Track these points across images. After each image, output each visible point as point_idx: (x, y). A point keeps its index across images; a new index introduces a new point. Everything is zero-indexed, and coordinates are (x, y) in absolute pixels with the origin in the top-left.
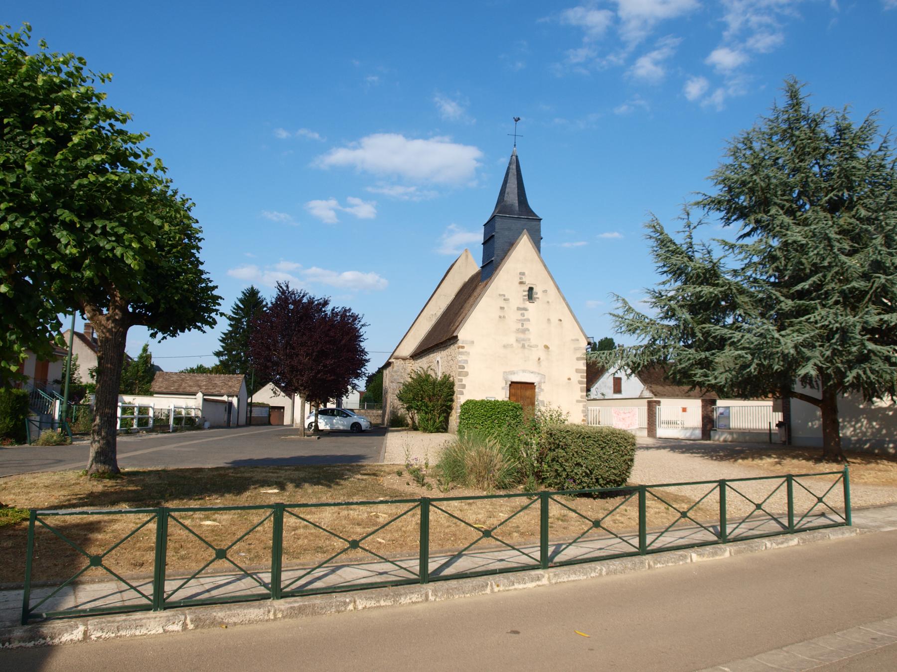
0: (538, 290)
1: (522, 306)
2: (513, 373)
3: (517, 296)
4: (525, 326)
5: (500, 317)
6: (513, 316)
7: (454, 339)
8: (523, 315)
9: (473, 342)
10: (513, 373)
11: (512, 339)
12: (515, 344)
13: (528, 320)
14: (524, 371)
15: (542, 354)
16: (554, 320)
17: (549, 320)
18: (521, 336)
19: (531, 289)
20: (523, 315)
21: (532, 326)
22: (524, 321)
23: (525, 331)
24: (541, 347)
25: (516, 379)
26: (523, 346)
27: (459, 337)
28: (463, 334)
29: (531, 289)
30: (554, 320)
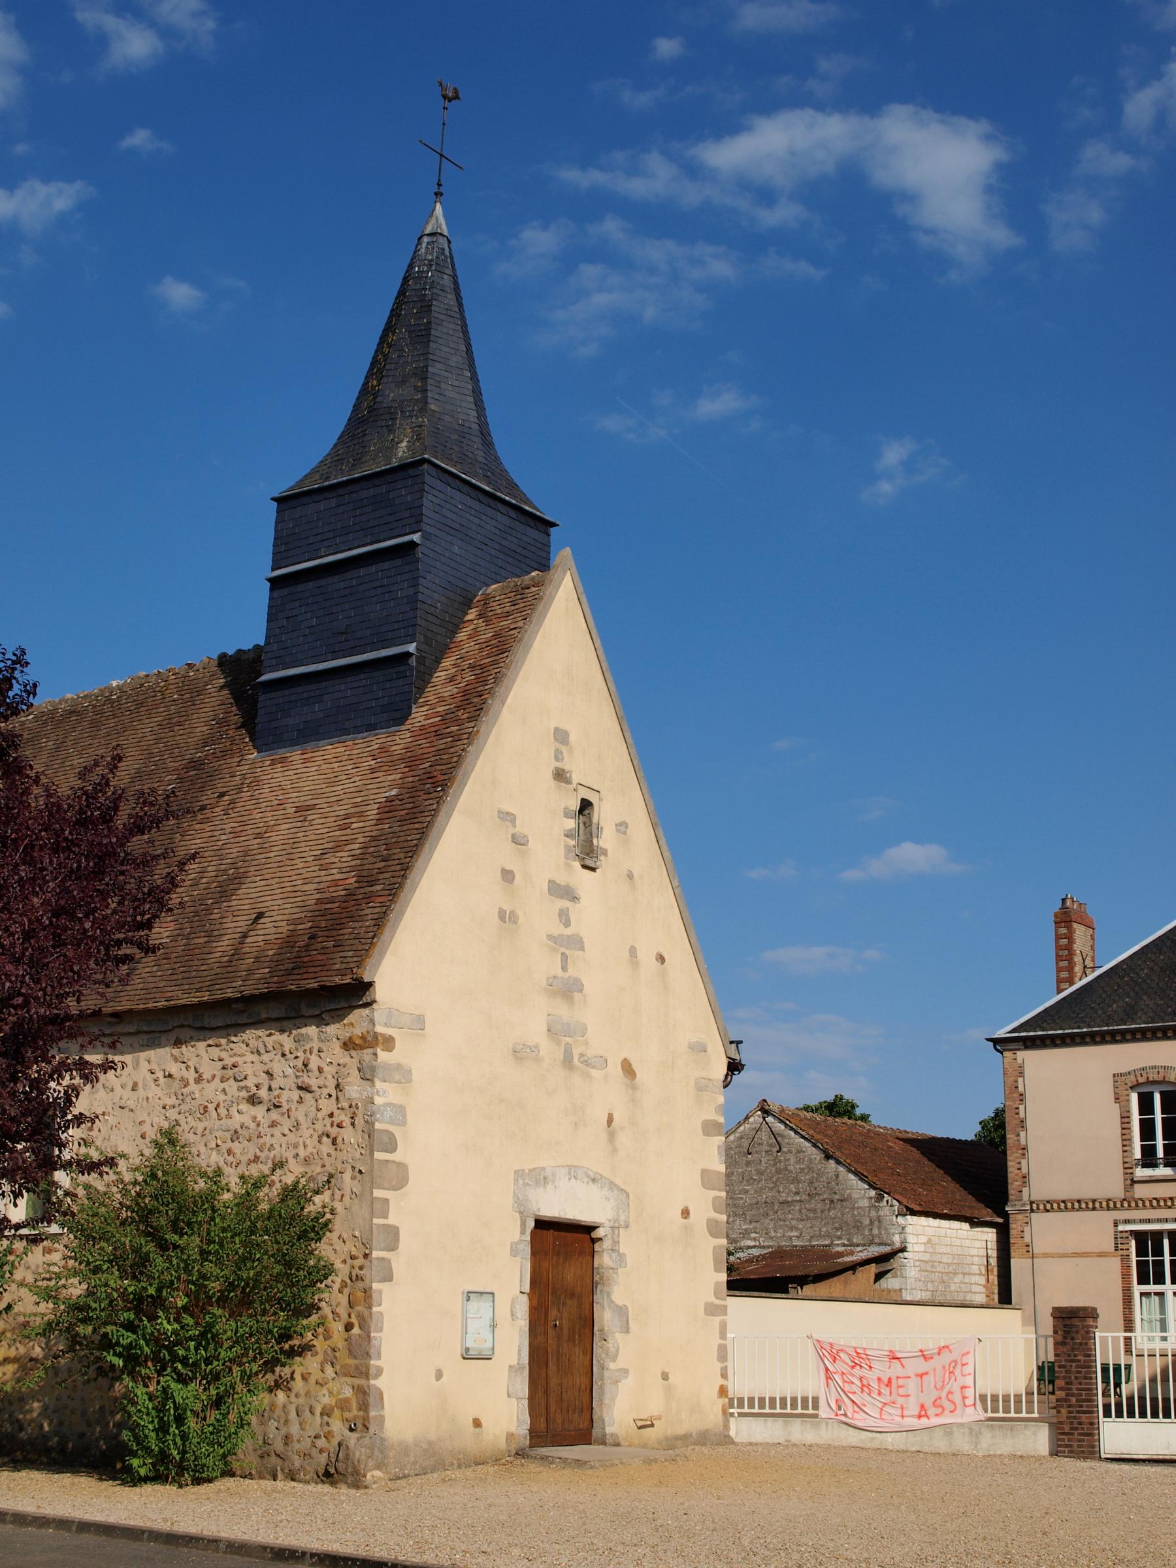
0: (603, 813)
1: (562, 880)
2: (540, 1178)
3: (550, 826)
4: (572, 972)
5: (502, 915)
6: (540, 917)
7: (357, 993)
8: (564, 918)
9: (419, 1023)
10: (540, 1178)
11: (535, 1032)
12: (549, 1051)
13: (577, 943)
14: (573, 1171)
15: (607, 1093)
16: (647, 958)
17: (633, 951)
18: (562, 1011)
19: (586, 805)
20: (564, 918)
21: (596, 972)
22: (567, 945)
23: (567, 990)
24: (615, 1068)
25: (553, 1210)
26: (568, 1062)
27: (383, 991)
28: (401, 971)
29: (586, 805)
30: (647, 958)
